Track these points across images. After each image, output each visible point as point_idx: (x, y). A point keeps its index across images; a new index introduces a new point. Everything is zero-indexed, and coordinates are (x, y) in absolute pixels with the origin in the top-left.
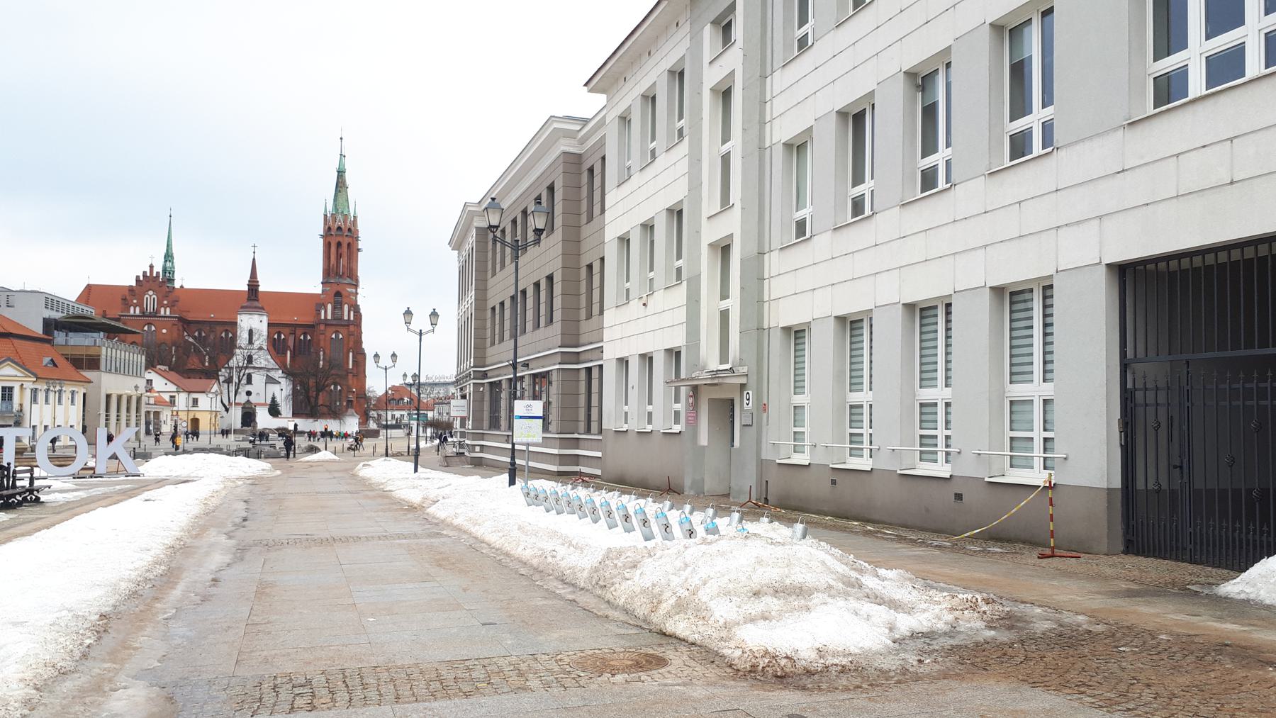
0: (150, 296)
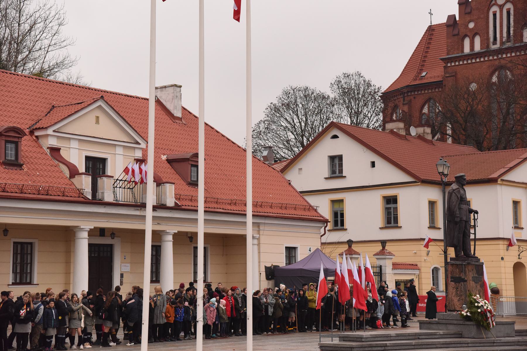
0: (501, 7)
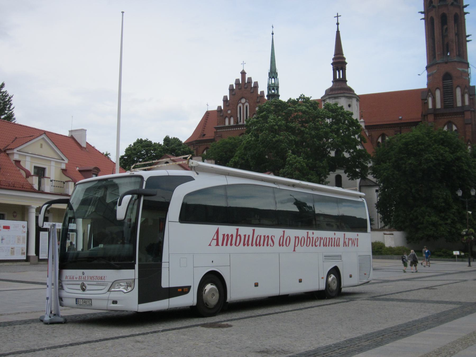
0: (243, 104)
